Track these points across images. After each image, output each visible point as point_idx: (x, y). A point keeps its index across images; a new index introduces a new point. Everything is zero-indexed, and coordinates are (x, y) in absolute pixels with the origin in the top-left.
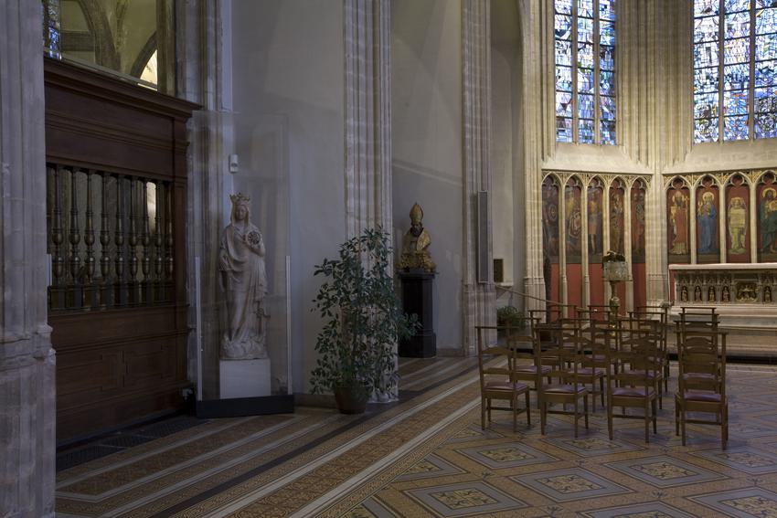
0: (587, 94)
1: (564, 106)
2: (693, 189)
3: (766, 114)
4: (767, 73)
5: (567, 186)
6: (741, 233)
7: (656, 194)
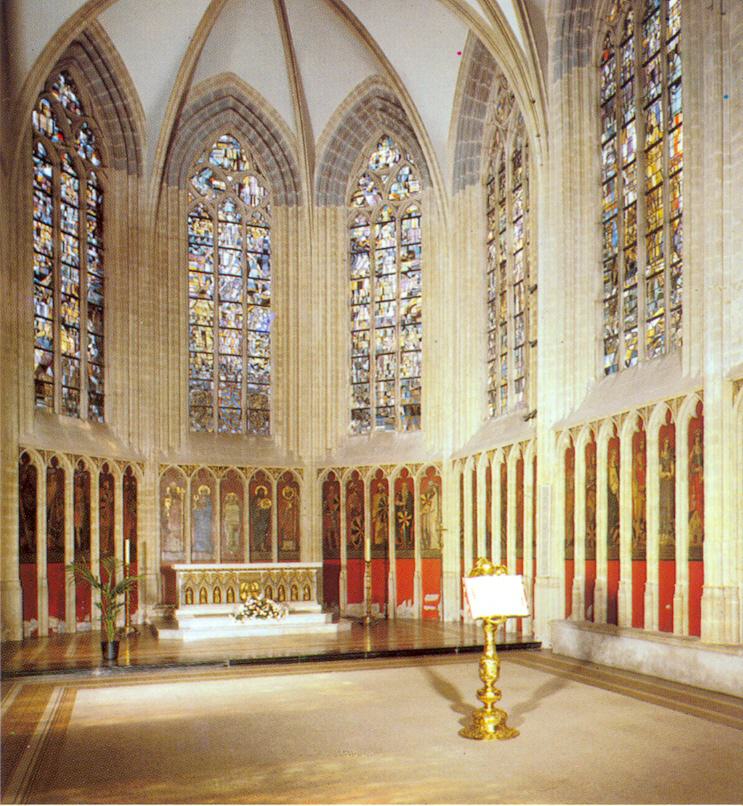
3: (257, 411)
4: (258, 370)
6: (235, 530)
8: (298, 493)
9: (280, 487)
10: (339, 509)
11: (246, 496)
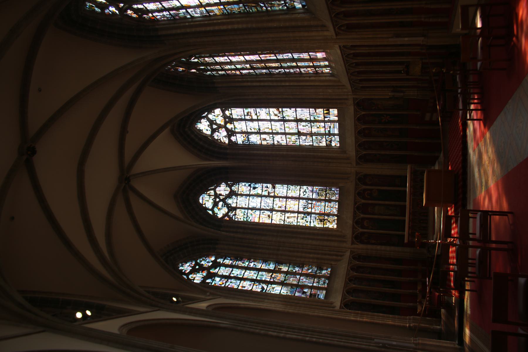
0: (299, 280)
1: (304, 293)
2: (361, 230)
3: (326, 194)
4: (306, 192)
5: (352, 297)
11: (370, 202)
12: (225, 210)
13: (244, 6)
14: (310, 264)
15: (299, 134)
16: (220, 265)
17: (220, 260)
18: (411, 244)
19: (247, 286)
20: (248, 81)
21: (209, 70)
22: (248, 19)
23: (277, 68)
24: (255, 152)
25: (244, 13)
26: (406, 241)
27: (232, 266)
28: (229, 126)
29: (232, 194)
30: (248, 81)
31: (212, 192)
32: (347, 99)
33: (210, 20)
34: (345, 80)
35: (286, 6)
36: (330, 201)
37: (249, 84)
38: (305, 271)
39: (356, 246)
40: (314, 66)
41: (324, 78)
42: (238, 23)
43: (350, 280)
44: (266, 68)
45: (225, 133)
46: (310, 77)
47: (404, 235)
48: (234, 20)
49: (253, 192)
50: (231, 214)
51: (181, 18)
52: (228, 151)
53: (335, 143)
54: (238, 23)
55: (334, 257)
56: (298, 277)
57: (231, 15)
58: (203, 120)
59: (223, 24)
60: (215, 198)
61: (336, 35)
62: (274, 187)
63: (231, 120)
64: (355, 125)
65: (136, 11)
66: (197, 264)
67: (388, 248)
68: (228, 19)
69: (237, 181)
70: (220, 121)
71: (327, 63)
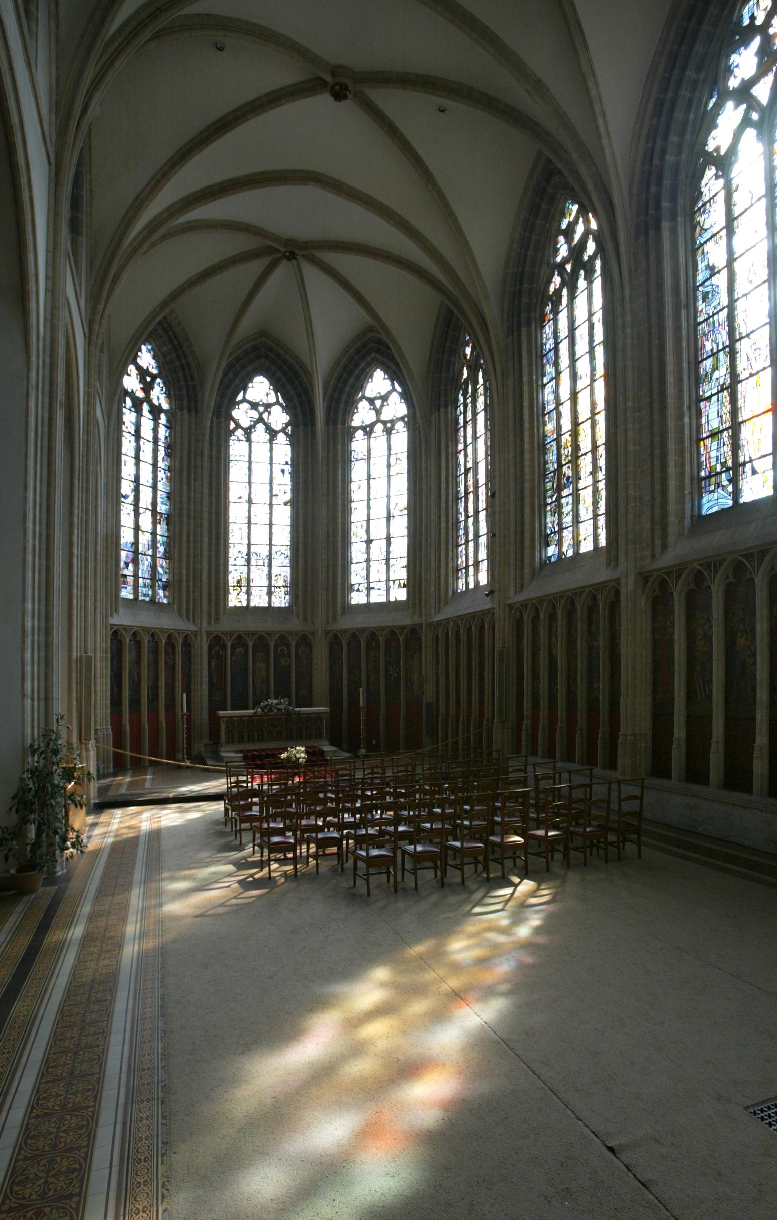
0: (145, 555)
1: (127, 565)
2: (229, 645)
5: (130, 641)
7: (202, 647)
8: (311, 651)
9: (297, 647)
10: (342, 664)
11: (272, 655)
12: (245, 423)
13: (554, 471)
14: (171, 570)
15: (369, 542)
16: (156, 419)
17: (163, 419)
18: (214, 721)
19: (127, 470)
20: (447, 462)
21: (465, 399)
22: (536, 475)
23: (466, 510)
24: (340, 472)
25: (545, 470)
26: (221, 713)
27: (156, 440)
28: (379, 428)
29: (273, 434)
30: (447, 462)
31: (272, 399)
32: (420, 615)
33: (538, 415)
34: (449, 612)
35: (552, 533)
36: (270, 593)
37: (444, 464)
38: (160, 562)
39: (204, 638)
40: (467, 567)
41: (450, 581)
42: (532, 460)
43: (153, 635)
44: (467, 493)
45: (368, 422)
46: (453, 559)
47: (226, 710)
48: (536, 453)
49: (277, 470)
50: (240, 433)
51: (543, 366)
52: (340, 426)
53: (357, 598)
54: (532, 460)
55: (185, 607)
56: (150, 552)
57: (543, 449)
58: (388, 382)
59: (532, 435)
60: (264, 404)
61: (509, 605)
62: (286, 504)
63: (388, 431)
64: (383, 628)
65: (558, 292)
66: (154, 377)
67: (205, 687)
68: (538, 444)
69: (294, 441)
70: (386, 415)
71: (472, 586)
